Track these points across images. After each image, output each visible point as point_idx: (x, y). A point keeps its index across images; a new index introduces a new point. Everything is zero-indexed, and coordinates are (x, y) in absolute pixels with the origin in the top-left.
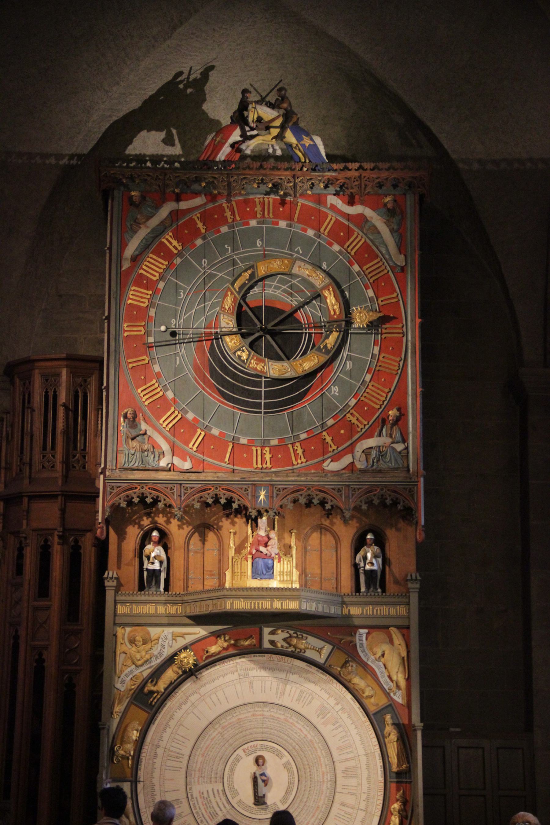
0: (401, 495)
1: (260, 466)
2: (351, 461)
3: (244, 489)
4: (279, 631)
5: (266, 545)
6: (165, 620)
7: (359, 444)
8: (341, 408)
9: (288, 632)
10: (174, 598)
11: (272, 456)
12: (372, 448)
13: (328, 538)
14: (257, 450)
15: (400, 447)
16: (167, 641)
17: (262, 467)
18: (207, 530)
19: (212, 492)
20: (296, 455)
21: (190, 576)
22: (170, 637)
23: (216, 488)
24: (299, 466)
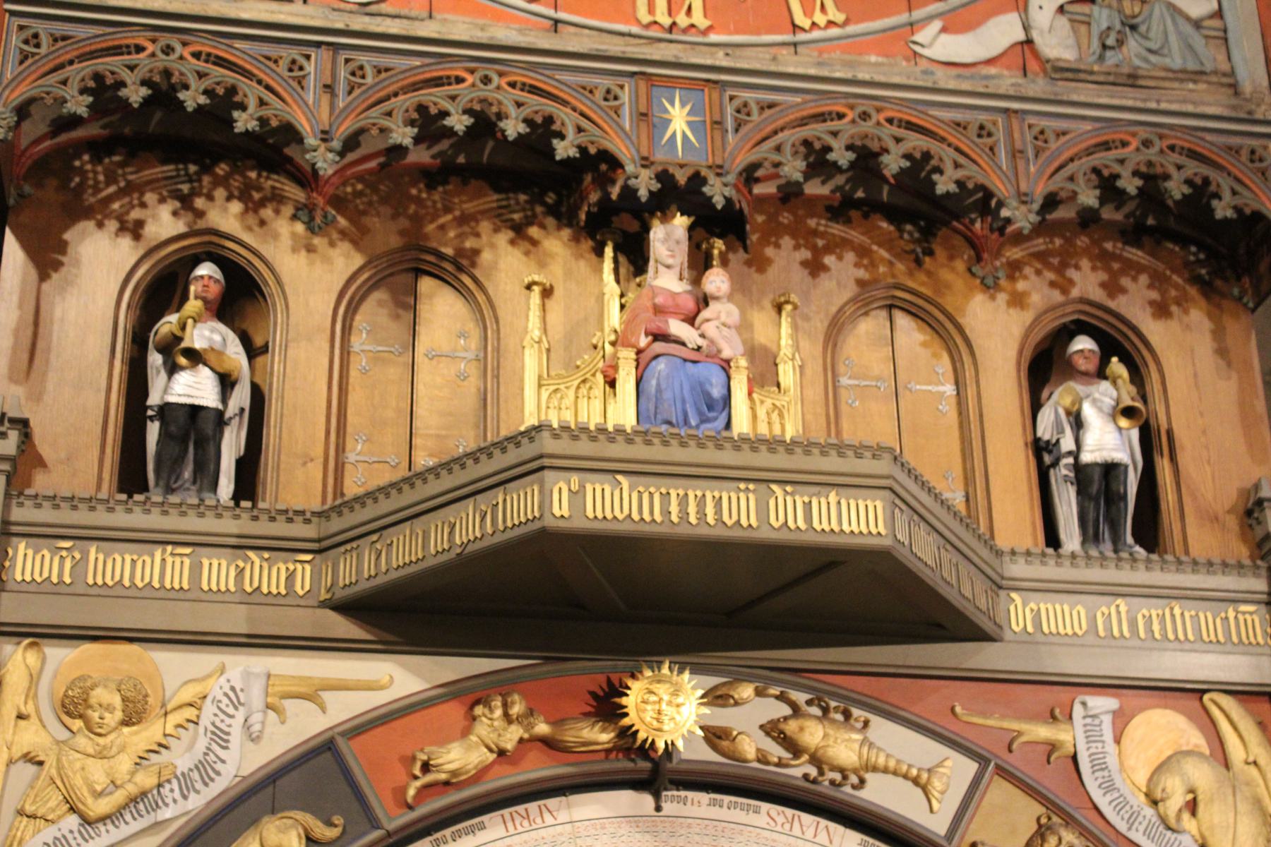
4: (746, 691)
5: (691, 320)
6: (236, 621)
9: (782, 697)
10: (280, 528)
16: (240, 715)
17: (674, 24)
18: (426, 285)
19: (469, 91)
21: (351, 457)
22: (256, 697)
24: (816, 34)
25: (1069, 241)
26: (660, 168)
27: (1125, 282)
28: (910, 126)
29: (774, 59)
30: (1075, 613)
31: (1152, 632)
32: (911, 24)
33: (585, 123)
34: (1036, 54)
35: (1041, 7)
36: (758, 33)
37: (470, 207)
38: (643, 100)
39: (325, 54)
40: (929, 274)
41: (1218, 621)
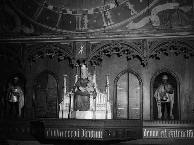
0: (188, 45)
1: (80, 29)
2: (148, 21)
13: (134, 80)
20: (107, 20)
26: (77, 60)
30: (156, 132)
31: (171, 135)
35: (153, 14)
41: (185, 133)
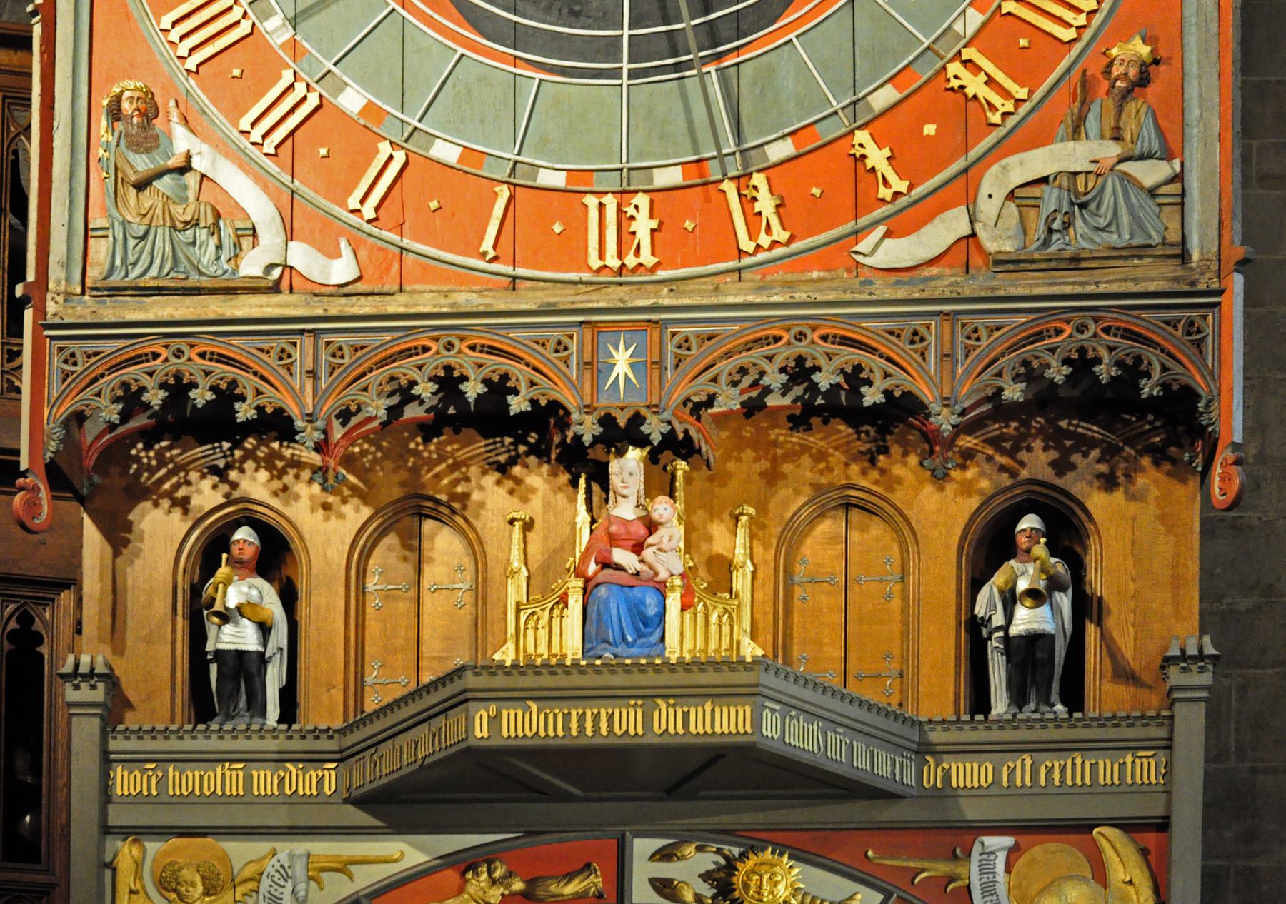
1: (614, 263)
3: (551, 345)
5: (638, 548)
7: (995, 168)
8: (927, 43)
11: (661, 224)
12: (1044, 180)
14: (601, 206)
15: (1151, 173)
17: (623, 265)
18: (429, 525)
19: (434, 361)
20: (753, 219)
23: (449, 346)
24: (761, 256)
25: (1025, 424)
27: (1076, 458)
28: (846, 341)
29: (717, 289)
32: (856, 233)
33: (537, 377)
34: (980, 248)
35: (990, 196)
36: (705, 264)
37: (462, 454)
38: (588, 349)
39: (308, 341)
40: (883, 472)
